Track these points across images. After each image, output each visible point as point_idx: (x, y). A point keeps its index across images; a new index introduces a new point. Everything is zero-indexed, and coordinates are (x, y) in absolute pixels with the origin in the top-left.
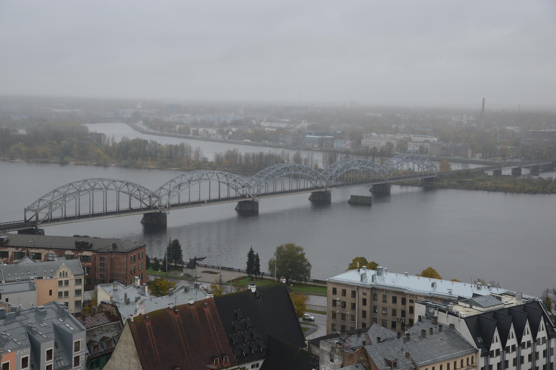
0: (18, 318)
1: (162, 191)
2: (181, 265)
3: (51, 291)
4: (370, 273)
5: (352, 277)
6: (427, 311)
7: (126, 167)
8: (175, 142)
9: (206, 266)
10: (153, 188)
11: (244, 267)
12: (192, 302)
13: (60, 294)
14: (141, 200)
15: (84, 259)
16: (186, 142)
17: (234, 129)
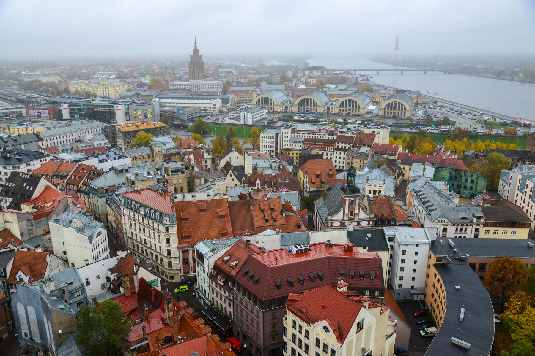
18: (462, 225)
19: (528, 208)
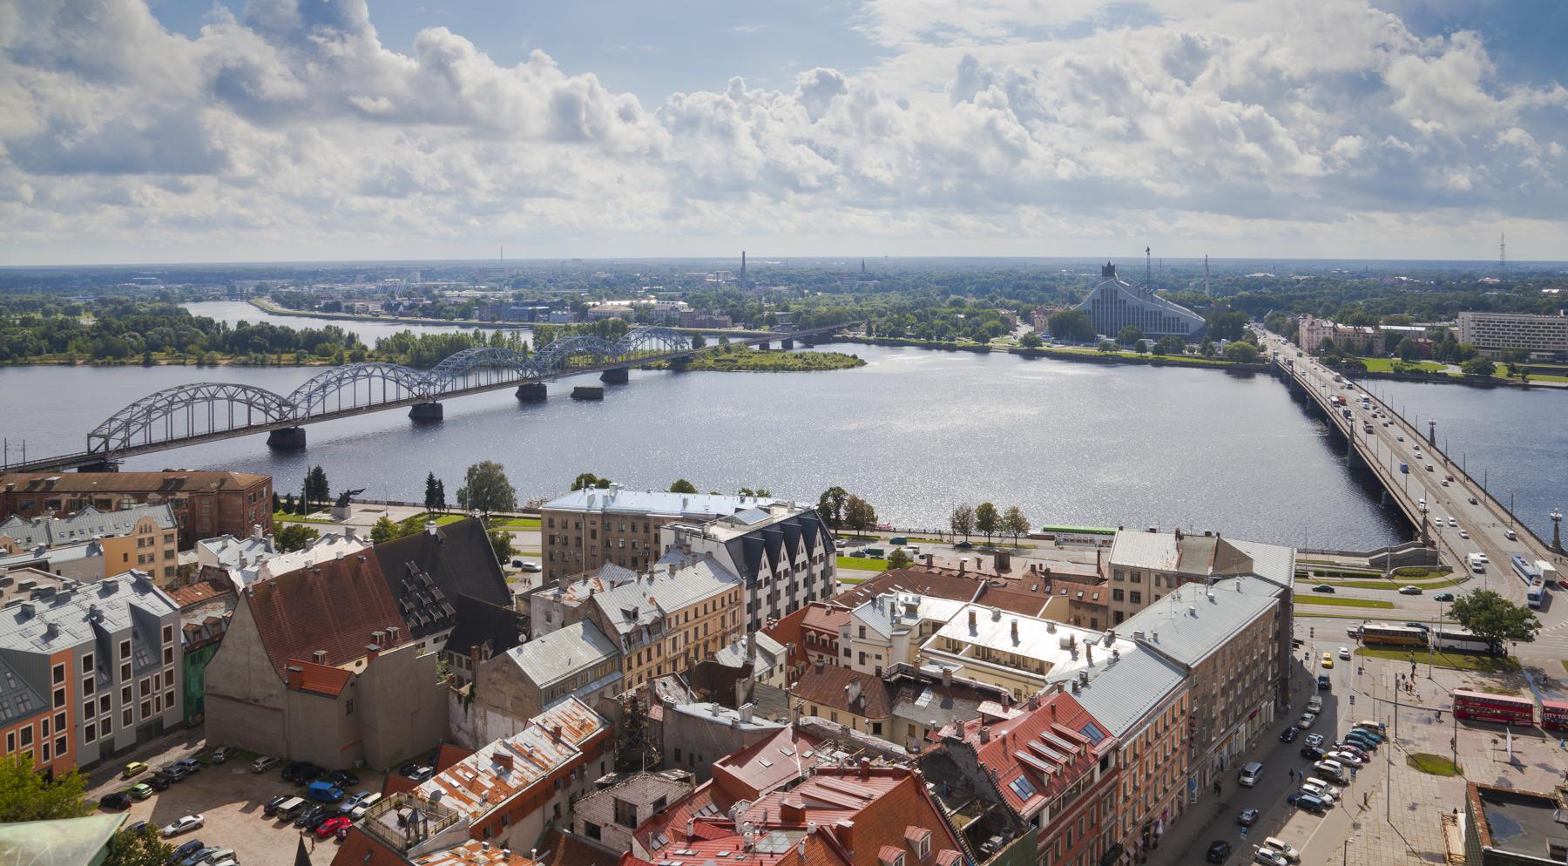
0: (74, 599)
4: (600, 494)
5: (577, 502)
6: (677, 538)
8: (318, 325)
9: (364, 502)
11: (422, 498)
13: (141, 560)
14: (266, 412)
16: (333, 323)
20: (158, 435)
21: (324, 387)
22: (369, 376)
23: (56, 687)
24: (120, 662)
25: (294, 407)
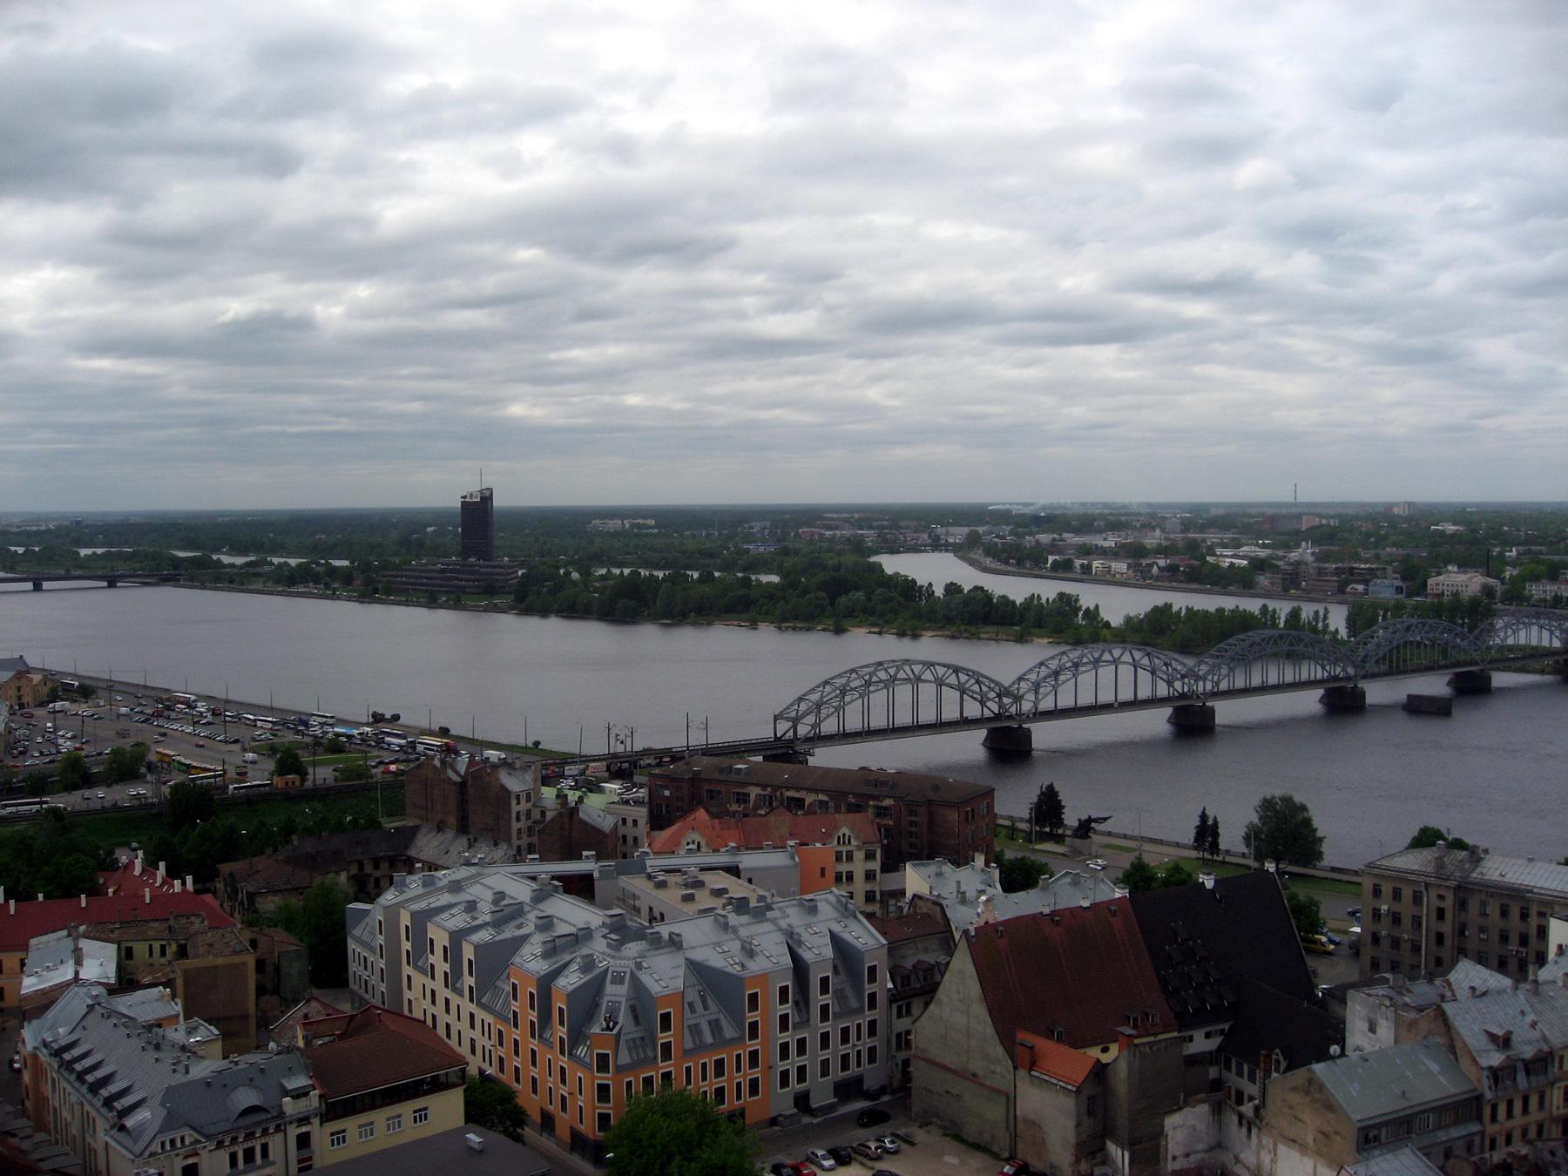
0: (769, 914)
1: (1023, 684)
2: (1060, 831)
3: (823, 870)
7: (953, 637)
8: (1048, 590)
10: (1007, 680)
11: (1189, 836)
12: (1086, 904)
14: (983, 703)
15: (881, 812)
17: (1162, 563)
18: (250, 1136)
19: (448, 1019)
20: (853, 722)
21: (1056, 674)
22: (1116, 662)
23: (751, 1017)
24: (818, 999)
25: (1018, 699)
